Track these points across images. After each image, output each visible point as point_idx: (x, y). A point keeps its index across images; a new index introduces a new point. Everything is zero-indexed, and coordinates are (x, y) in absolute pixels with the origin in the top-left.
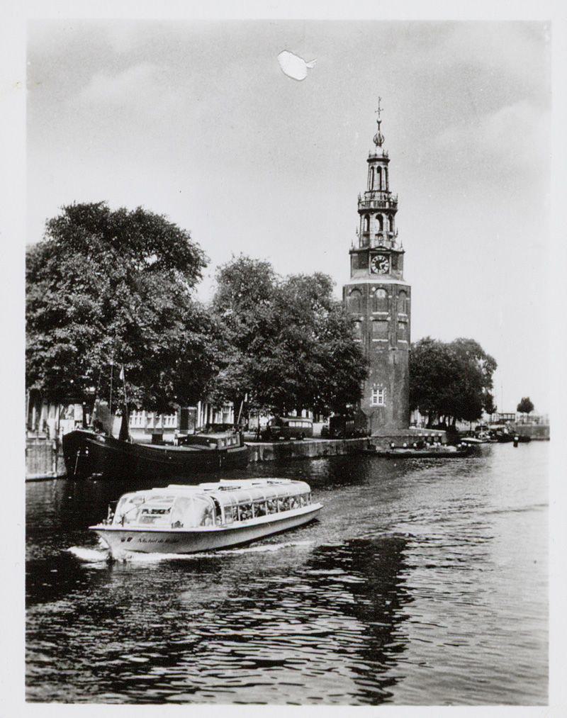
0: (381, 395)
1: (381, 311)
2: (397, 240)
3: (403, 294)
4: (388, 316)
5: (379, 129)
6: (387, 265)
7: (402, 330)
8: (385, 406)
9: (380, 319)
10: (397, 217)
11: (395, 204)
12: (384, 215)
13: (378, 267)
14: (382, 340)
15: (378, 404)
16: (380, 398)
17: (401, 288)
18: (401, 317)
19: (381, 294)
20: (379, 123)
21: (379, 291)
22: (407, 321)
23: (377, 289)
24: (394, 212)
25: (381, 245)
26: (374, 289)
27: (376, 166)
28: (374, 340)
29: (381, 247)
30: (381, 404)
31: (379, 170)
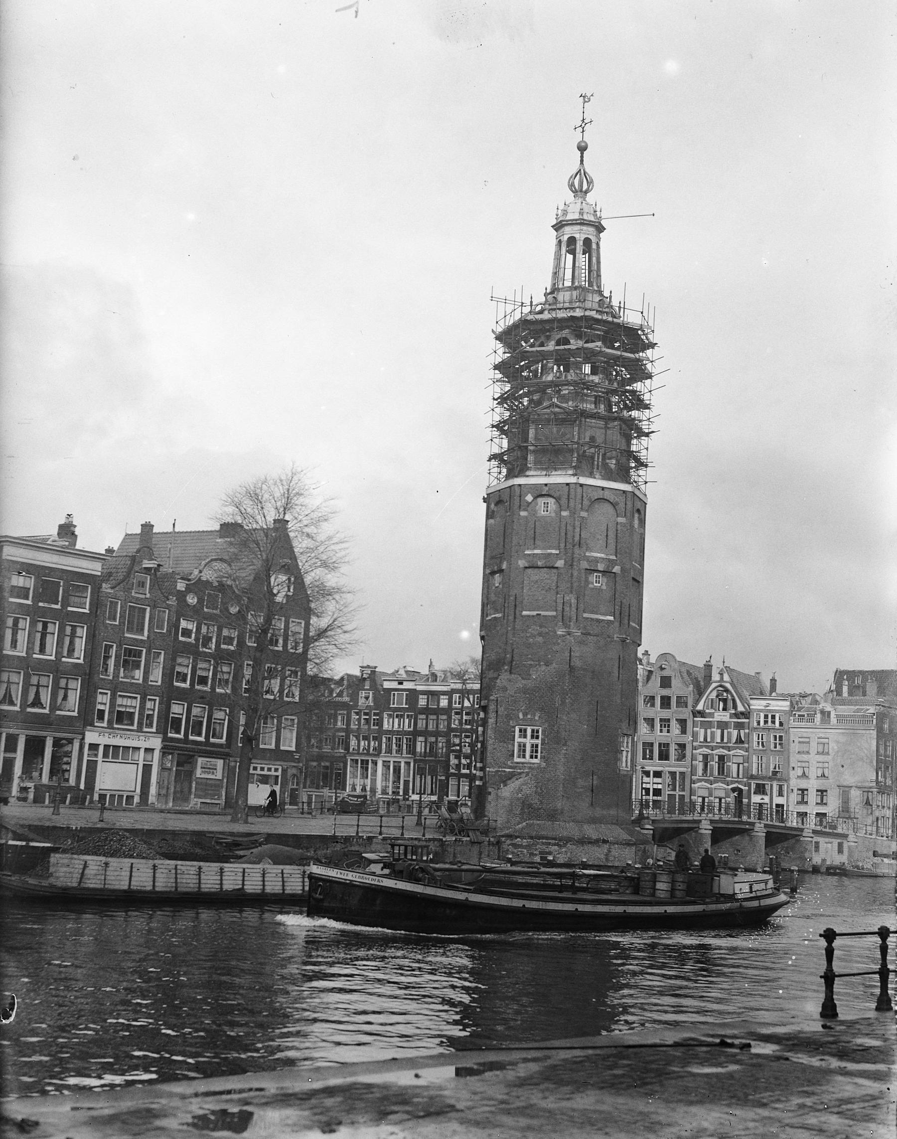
5: (582, 161)
7: (599, 590)
9: (540, 564)
16: (534, 747)
17: (600, 494)
18: (597, 560)
19: (546, 508)
20: (582, 148)
21: (541, 501)
27: (566, 238)
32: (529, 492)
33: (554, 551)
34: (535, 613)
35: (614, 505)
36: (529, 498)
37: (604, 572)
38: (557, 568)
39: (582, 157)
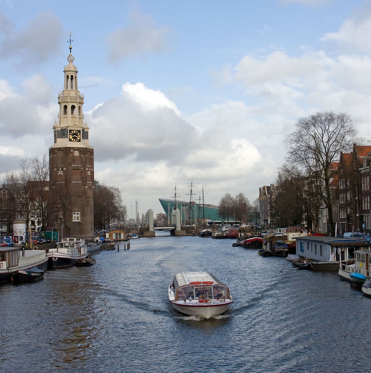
0: (78, 216)
1: (76, 165)
2: (84, 121)
3: (89, 153)
5: (71, 52)
7: (89, 175)
8: (81, 222)
10: (84, 107)
11: (83, 99)
15: (76, 221)
19: (77, 154)
20: (71, 49)
21: (75, 152)
22: (92, 170)
24: (82, 103)
25: (75, 124)
26: (72, 151)
28: (73, 182)
29: (75, 125)
30: (78, 221)
31: (72, 79)
33: (80, 165)
34: (75, 182)
39: (71, 51)
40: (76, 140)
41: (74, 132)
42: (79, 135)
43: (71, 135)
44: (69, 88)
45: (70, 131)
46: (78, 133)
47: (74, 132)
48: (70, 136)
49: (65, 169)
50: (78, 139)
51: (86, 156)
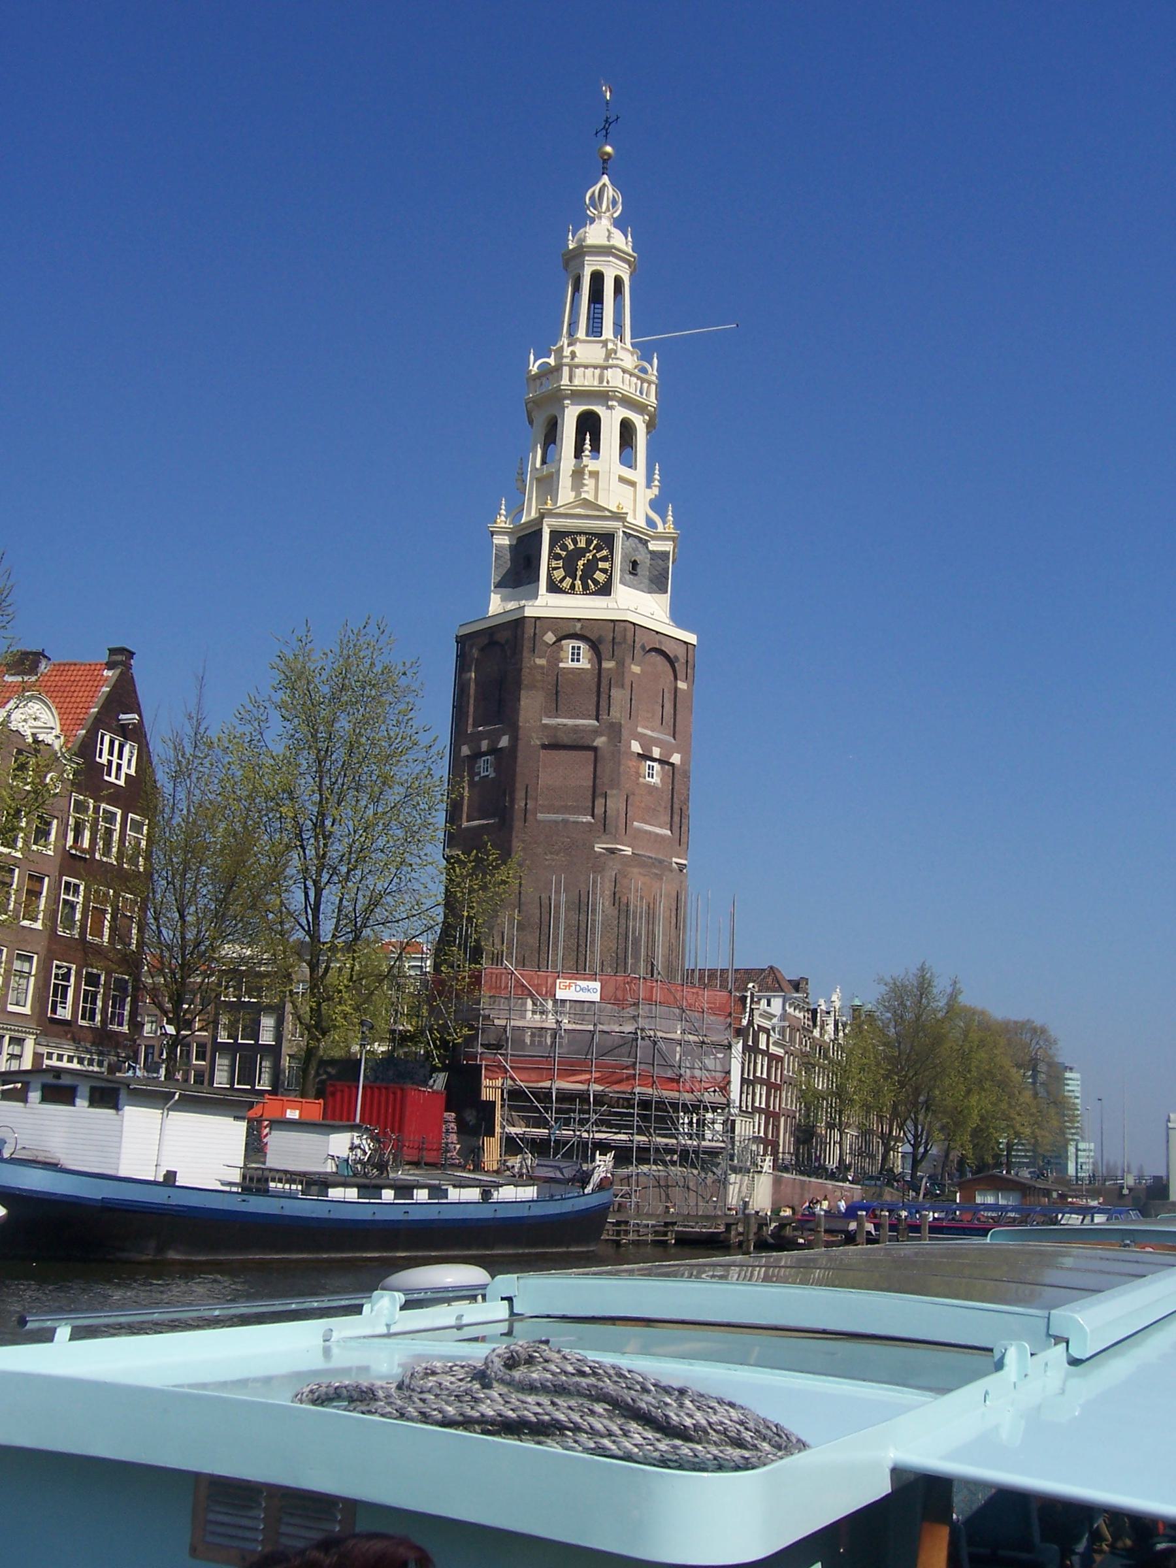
4: (596, 732)
6: (606, 565)
7: (651, 788)
9: (566, 740)
12: (599, 409)
13: (571, 572)
14: (572, 818)
22: (676, 759)
23: (559, 640)
32: (549, 630)
34: (560, 817)
35: (671, 661)
36: (550, 638)
37: (659, 761)
38: (595, 749)
40: (585, 587)
41: (575, 542)
42: (605, 559)
43: (557, 557)
44: (581, 334)
45: (557, 536)
46: (599, 548)
47: (575, 542)
48: (554, 564)
49: (504, 742)
50: (596, 582)
51: (636, 669)
